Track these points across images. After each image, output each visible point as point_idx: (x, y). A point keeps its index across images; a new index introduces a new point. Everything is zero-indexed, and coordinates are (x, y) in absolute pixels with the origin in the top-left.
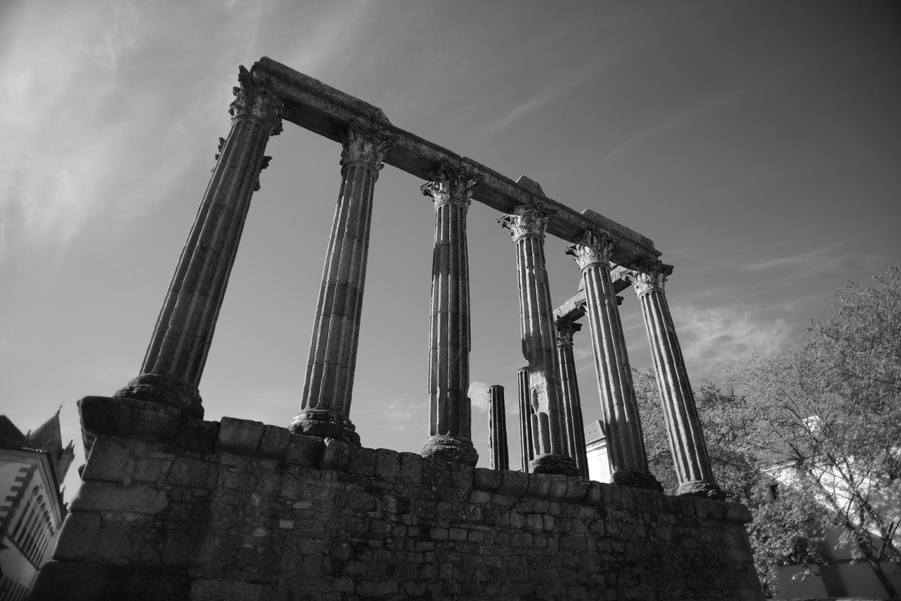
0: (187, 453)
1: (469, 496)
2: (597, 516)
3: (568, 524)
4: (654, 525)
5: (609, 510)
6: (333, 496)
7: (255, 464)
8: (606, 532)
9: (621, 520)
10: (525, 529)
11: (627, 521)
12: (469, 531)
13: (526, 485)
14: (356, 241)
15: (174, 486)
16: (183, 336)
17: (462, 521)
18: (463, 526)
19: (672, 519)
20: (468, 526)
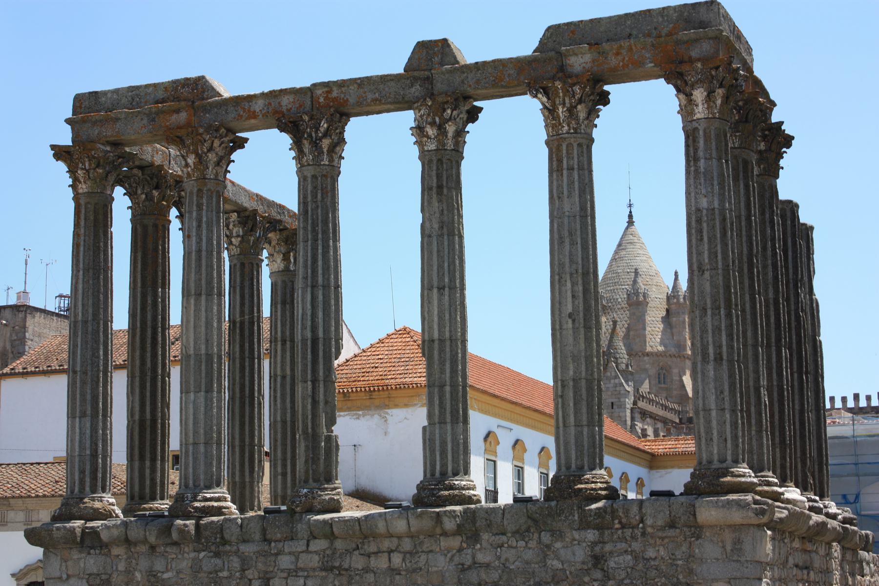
0: (92, 551)
1: (308, 545)
2: (465, 545)
3: (423, 557)
4: (558, 545)
5: (485, 536)
6: (190, 565)
7: (132, 550)
8: (475, 563)
9: (501, 546)
10: (367, 570)
11: (510, 547)
12: (306, 577)
13: (358, 528)
14: (192, 301)
15: (90, 575)
16: (77, 459)
17: (302, 569)
18: (301, 574)
19: (591, 535)
20: (306, 574)
